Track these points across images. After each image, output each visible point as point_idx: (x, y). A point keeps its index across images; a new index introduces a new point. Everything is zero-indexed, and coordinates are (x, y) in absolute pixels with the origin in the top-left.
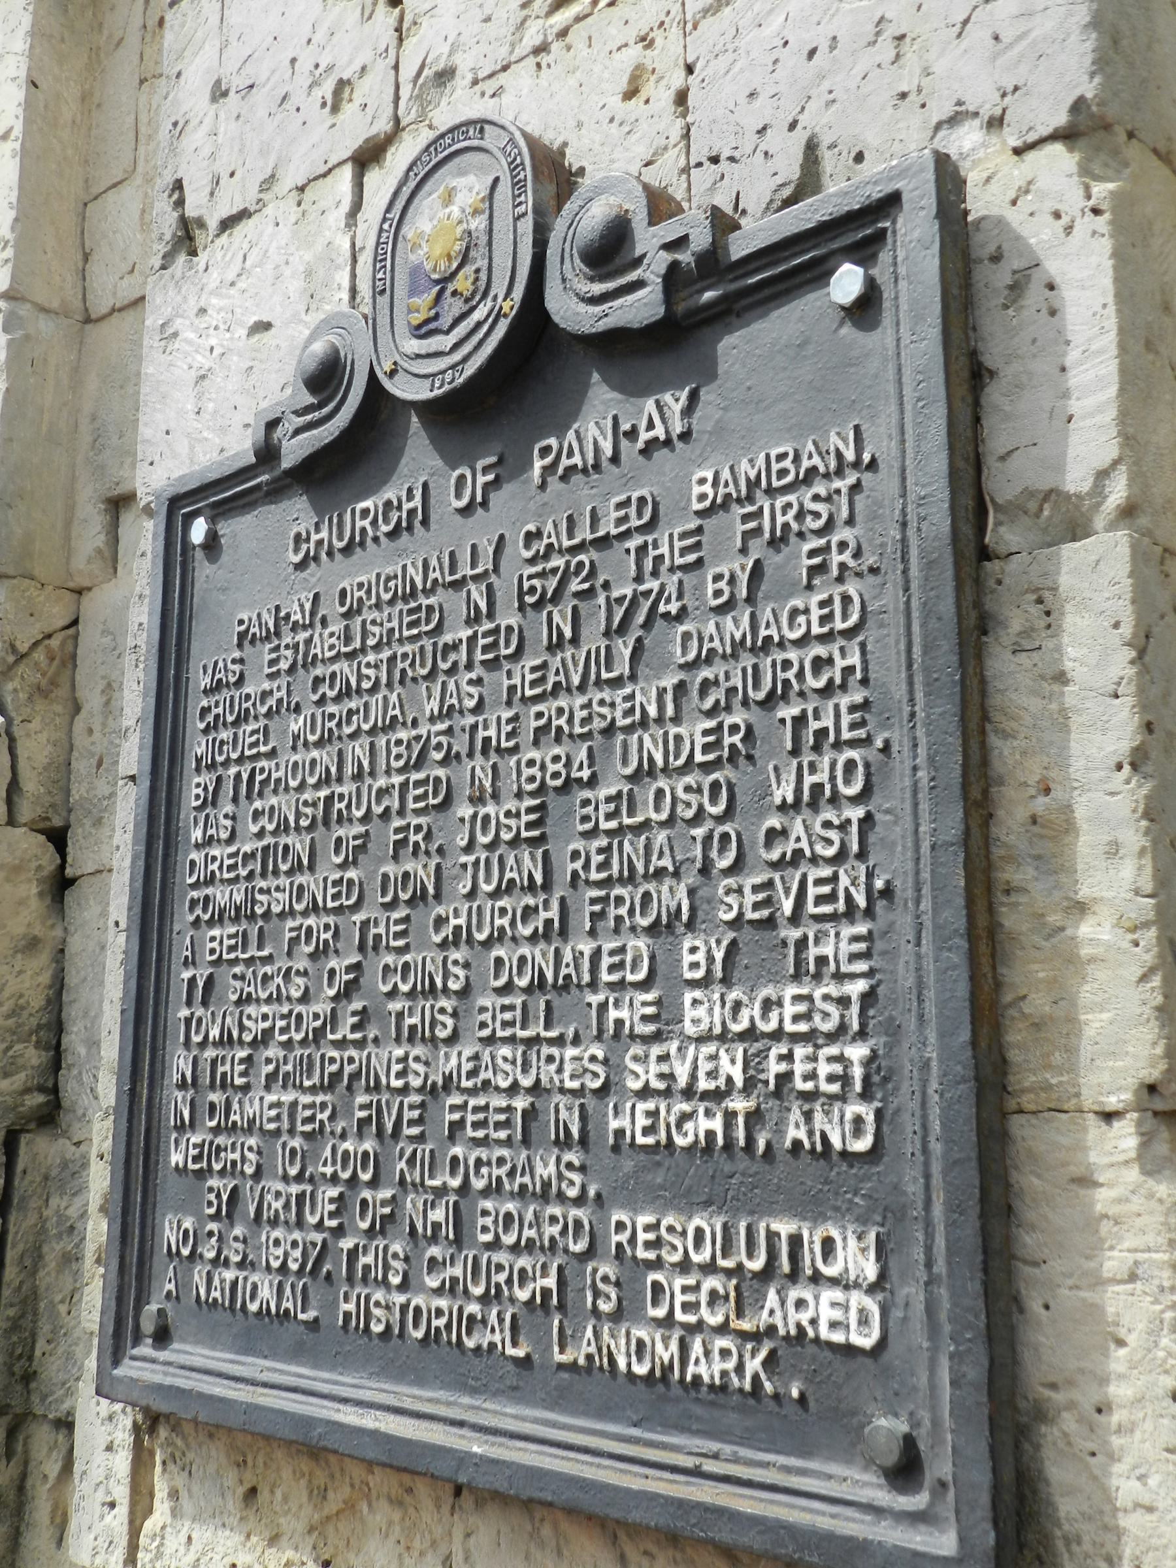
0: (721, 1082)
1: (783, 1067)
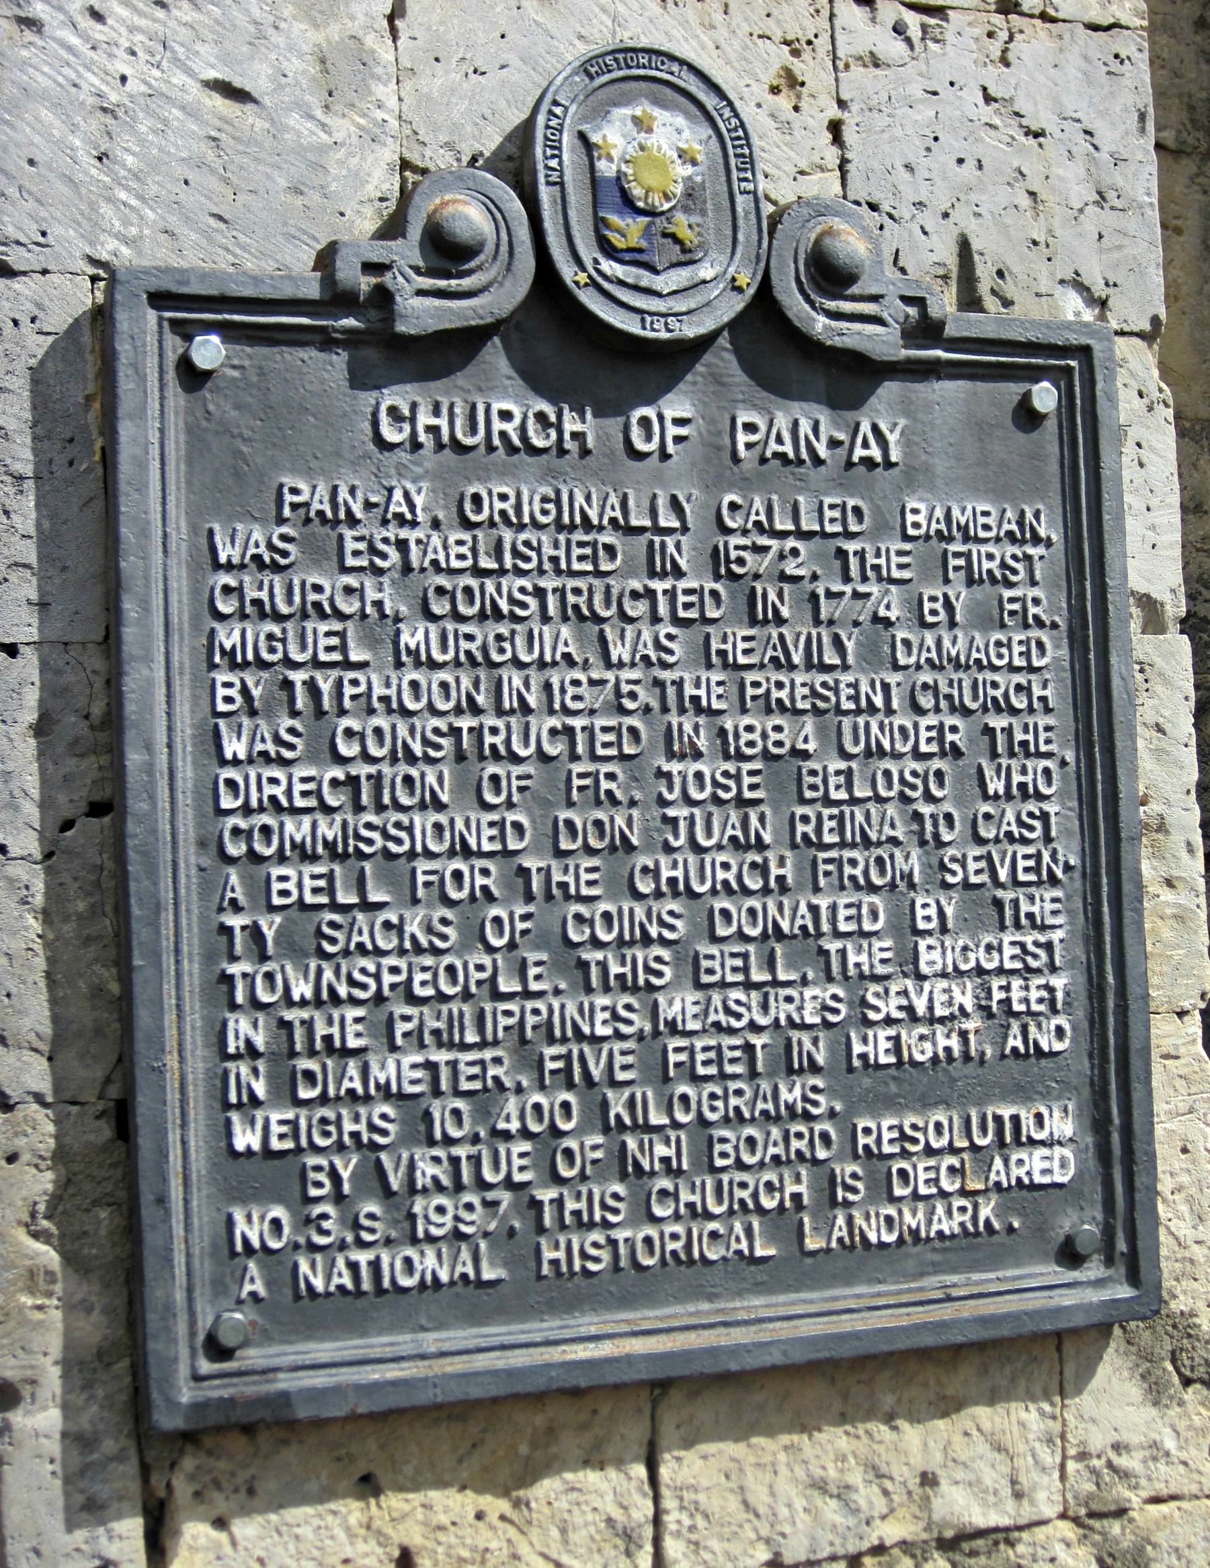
1: (1003, 995)
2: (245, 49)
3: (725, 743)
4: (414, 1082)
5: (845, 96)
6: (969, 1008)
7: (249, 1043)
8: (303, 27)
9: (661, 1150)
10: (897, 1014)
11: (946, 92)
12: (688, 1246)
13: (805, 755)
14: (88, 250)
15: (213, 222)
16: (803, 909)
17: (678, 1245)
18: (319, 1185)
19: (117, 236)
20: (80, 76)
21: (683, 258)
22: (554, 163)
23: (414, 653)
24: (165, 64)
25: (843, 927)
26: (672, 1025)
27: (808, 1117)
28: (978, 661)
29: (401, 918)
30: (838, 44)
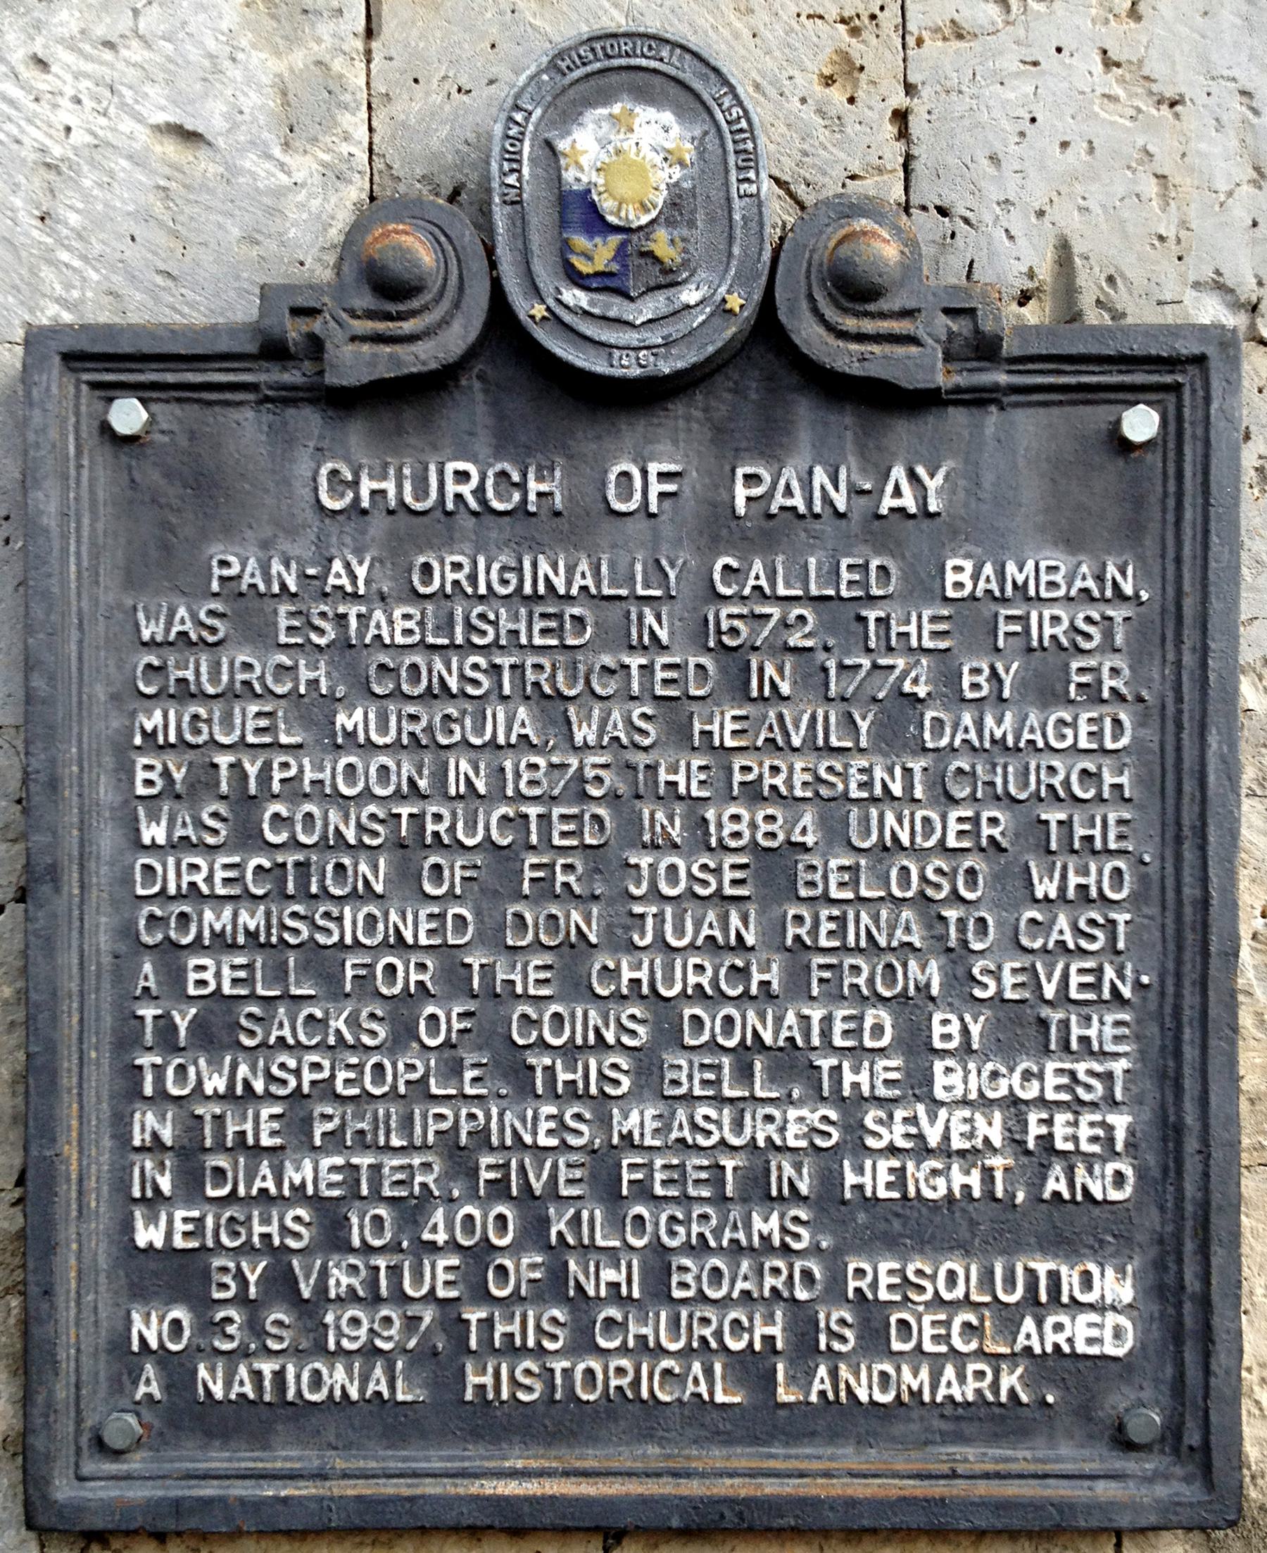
0: (978, 1143)
1: (1044, 1130)
2: (198, 86)
3: (707, 833)
4: (330, 1186)
5: (911, 79)
6: (997, 1142)
7: (155, 1136)
8: (263, 56)
9: (608, 1275)
10: (901, 1143)
11: (1050, 61)
12: (636, 1383)
13: (803, 847)
14: (27, 317)
15: (159, 280)
16: (791, 1018)
17: (625, 1382)
18: (224, 1286)
19: (58, 300)
20: (23, 131)
21: (662, 280)
22: (511, 180)
23: (351, 735)
24: (112, 110)
25: (838, 1042)
26: (627, 1138)
27: (785, 1247)
28: (1031, 742)
29: (327, 1013)
30: (908, 15)
